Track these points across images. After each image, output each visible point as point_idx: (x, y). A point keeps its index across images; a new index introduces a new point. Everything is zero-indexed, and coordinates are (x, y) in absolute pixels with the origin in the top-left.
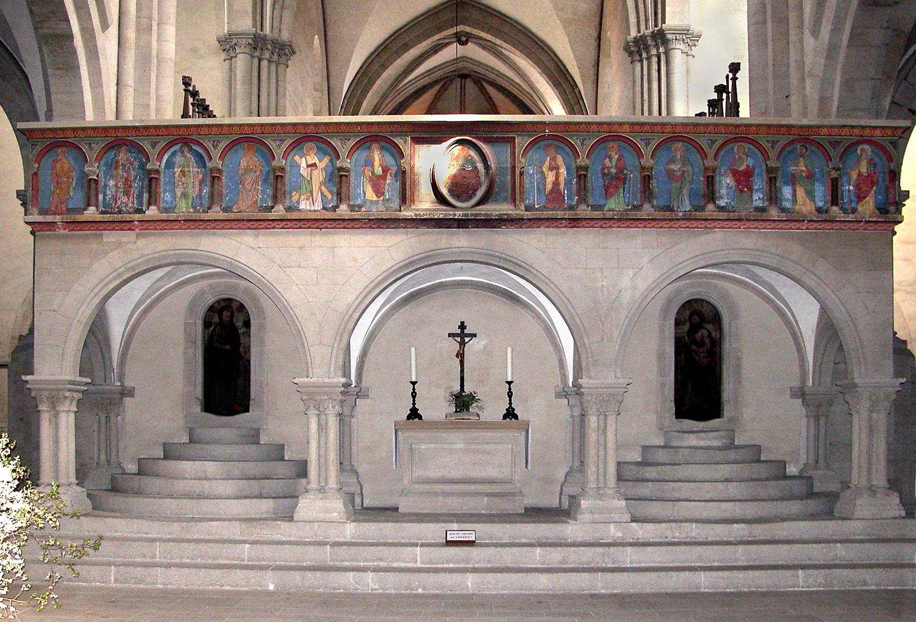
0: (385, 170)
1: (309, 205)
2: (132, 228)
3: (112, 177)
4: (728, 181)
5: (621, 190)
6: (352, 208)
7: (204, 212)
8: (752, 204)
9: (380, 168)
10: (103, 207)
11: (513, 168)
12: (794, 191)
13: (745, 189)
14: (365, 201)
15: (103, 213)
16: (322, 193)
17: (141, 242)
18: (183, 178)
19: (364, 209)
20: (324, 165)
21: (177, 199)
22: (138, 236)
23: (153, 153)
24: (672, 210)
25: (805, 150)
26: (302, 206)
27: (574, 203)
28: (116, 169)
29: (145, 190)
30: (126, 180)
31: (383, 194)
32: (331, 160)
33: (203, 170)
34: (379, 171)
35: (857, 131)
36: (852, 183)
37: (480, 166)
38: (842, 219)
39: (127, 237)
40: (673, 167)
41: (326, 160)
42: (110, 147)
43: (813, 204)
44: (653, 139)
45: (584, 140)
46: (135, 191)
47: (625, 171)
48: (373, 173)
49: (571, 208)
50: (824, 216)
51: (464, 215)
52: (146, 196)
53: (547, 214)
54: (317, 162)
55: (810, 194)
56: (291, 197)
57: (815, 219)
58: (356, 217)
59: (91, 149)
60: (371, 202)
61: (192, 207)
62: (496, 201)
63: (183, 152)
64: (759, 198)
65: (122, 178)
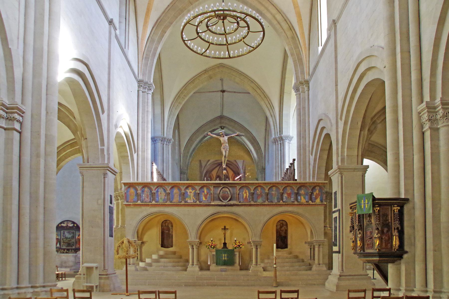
0: (207, 193)
1: (190, 201)
3: (144, 194)
4: (286, 195)
6: (200, 202)
11: (237, 193)
12: (301, 197)
15: (142, 202)
23: (153, 189)
24: (273, 202)
26: (188, 201)
27: (250, 201)
35: (316, 184)
37: (229, 192)
39: (148, 208)
40: (273, 192)
41: (194, 191)
42: (143, 187)
46: (149, 198)
49: (250, 202)
50: (308, 203)
52: (152, 198)
55: (305, 198)
60: (204, 200)
62: (233, 200)
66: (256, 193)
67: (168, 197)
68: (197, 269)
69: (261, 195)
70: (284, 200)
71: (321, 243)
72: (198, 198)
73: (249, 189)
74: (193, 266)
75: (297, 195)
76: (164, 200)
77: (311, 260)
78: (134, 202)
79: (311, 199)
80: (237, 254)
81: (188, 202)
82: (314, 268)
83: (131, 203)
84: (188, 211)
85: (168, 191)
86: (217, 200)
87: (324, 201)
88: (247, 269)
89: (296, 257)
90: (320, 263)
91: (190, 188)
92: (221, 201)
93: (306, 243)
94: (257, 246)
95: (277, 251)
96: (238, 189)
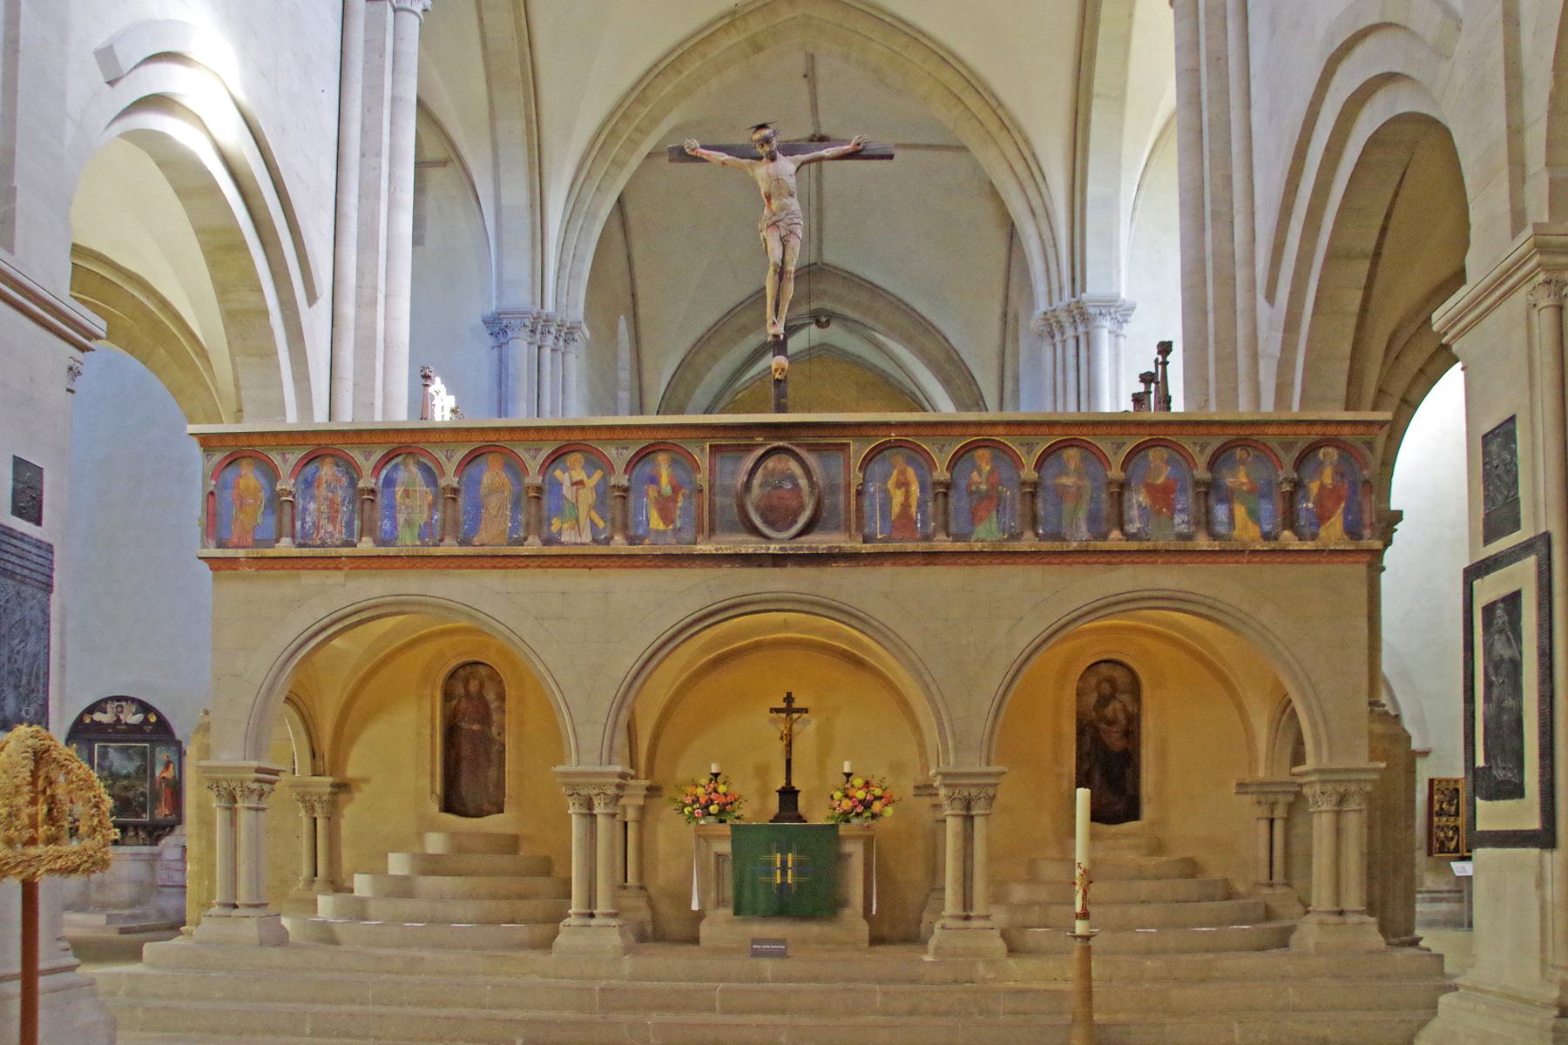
1: (574, 537)
2: (340, 566)
3: (313, 498)
4: (1141, 499)
5: (994, 514)
6: (632, 541)
7: (435, 545)
9: (669, 488)
10: (302, 538)
11: (849, 485)
14: (648, 532)
15: (301, 546)
16: (592, 521)
17: (352, 585)
18: (407, 501)
19: (647, 541)
20: (595, 483)
21: (399, 528)
22: (346, 576)
24: (1064, 540)
26: (564, 538)
27: (930, 530)
28: (318, 487)
29: (356, 516)
30: (332, 502)
31: (673, 522)
32: (604, 478)
33: (433, 489)
34: (666, 489)
36: (1312, 499)
37: (803, 482)
40: (1064, 480)
41: (598, 475)
42: (309, 459)
43: (1257, 529)
45: (944, 445)
46: (343, 518)
47: (1000, 488)
48: (659, 492)
50: (1273, 545)
51: (781, 549)
52: (357, 523)
53: (891, 547)
54: (585, 479)
55: (1253, 515)
56: (550, 525)
57: (1258, 547)
58: (636, 552)
59: (285, 461)
60: (657, 532)
61: (419, 539)
62: (824, 529)
63: (406, 466)
65: (326, 499)
66: (963, 483)
67: (449, 512)
68: (611, 937)
69: (990, 500)
70: (1132, 528)
71: (1353, 788)
72: (618, 523)
73: (923, 461)
74: (593, 922)
75: (1207, 494)
76: (425, 532)
77: (1271, 886)
78: (257, 544)
79: (1290, 521)
80: (855, 850)
81: (562, 544)
82: (1309, 933)
83: (241, 553)
84: (563, 593)
85: (450, 479)
86: (732, 528)
87: (1367, 532)
88: (914, 938)
89: (1191, 869)
90: (1345, 906)
91: (576, 459)
92: (753, 530)
93: (1242, 787)
94: (968, 805)
95: (1093, 837)
96: (856, 462)
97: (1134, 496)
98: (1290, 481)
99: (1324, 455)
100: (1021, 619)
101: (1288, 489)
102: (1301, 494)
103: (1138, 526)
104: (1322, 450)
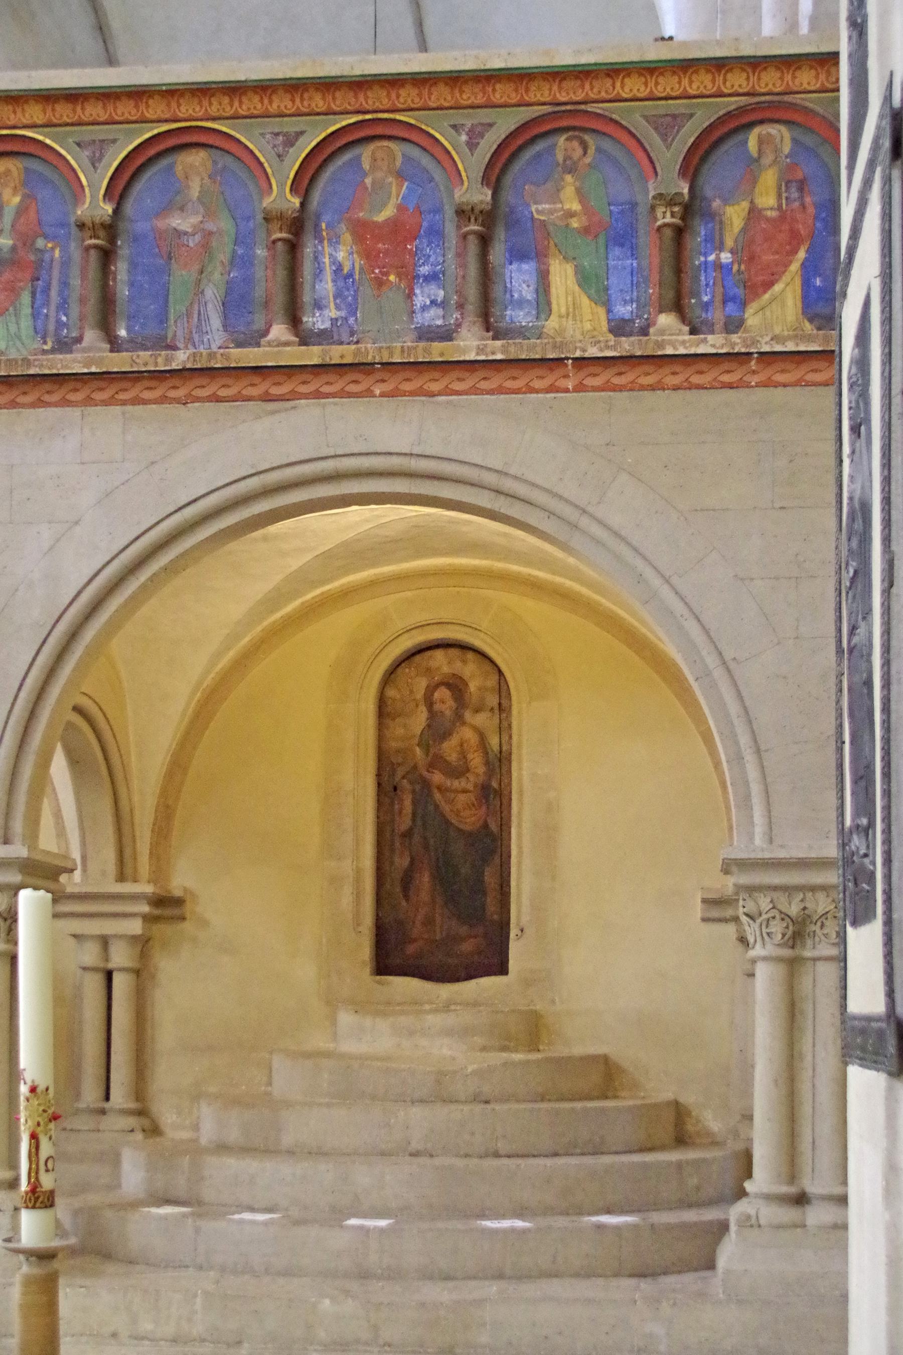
4: (341, 255)
8: (412, 322)
12: (543, 278)
13: (392, 278)
25: (579, 151)
36: (729, 242)
38: (682, 351)
40: (178, 222)
43: (601, 312)
44: (114, 141)
47: (40, 243)
50: (628, 346)
64: (433, 302)
70: (316, 321)
75: (485, 241)
97: (327, 250)
98: (671, 201)
99: (761, 141)
100: (77, 523)
101: (668, 219)
102: (701, 230)
103: (333, 313)
104: (756, 131)
